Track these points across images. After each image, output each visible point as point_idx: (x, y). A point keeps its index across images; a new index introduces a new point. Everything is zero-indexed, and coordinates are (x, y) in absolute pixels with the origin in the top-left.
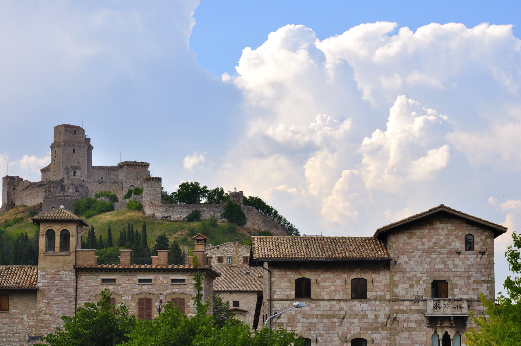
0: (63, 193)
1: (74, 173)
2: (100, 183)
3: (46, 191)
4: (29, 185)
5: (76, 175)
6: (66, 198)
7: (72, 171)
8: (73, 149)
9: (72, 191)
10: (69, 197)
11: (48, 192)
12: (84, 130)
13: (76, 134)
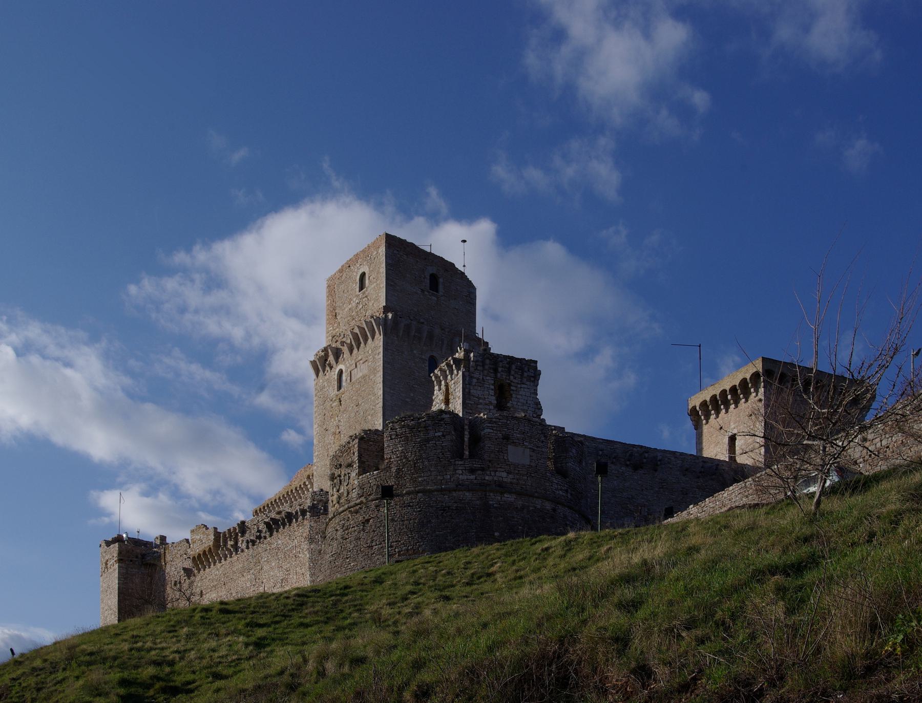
0: (472, 471)
1: (502, 393)
2: (636, 468)
3: (350, 465)
4: (211, 543)
5: (509, 405)
6: (494, 499)
7: (490, 380)
8: (426, 356)
9: (527, 462)
10: (509, 498)
11: (359, 474)
12: (474, 289)
13: (441, 294)
